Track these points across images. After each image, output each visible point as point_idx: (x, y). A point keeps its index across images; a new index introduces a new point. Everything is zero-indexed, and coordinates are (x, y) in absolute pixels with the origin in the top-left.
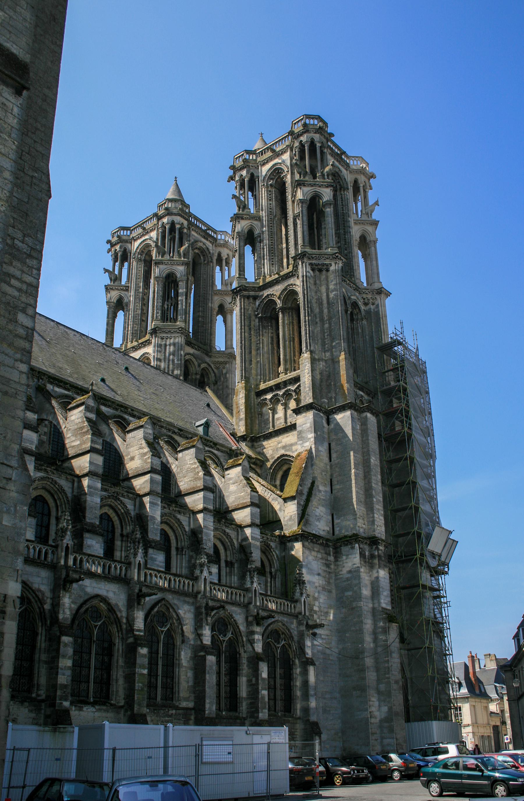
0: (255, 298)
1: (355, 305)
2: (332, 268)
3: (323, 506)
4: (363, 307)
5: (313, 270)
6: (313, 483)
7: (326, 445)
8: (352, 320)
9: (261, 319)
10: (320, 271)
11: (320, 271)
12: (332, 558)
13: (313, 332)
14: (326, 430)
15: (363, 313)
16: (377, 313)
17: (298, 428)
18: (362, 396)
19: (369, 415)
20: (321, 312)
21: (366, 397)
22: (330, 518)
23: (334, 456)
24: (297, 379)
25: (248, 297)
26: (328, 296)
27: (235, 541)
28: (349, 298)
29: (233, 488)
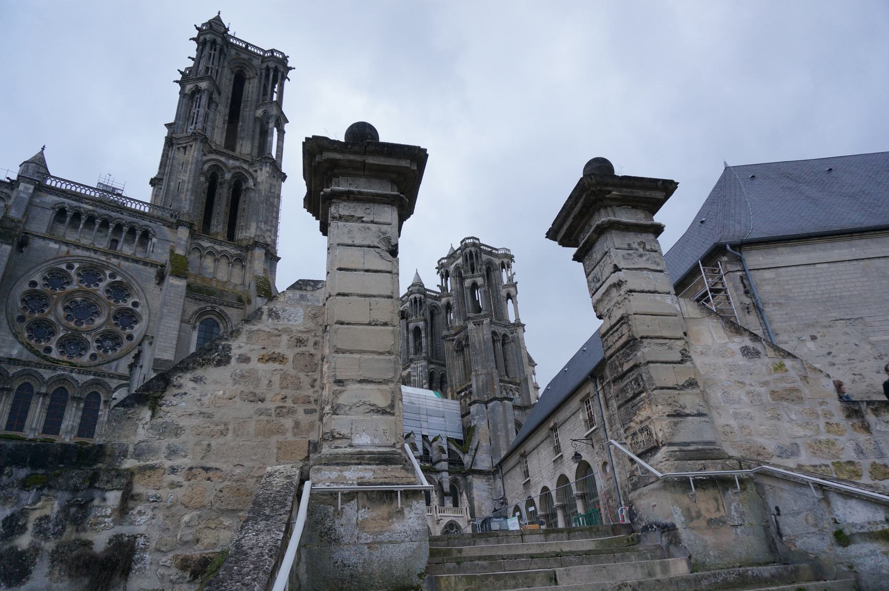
0: (453, 340)
1: (505, 336)
2: (484, 323)
3: (485, 453)
4: (510, 336)
5: (475, 325)
6: (479, 442)
7: (486, 420)
8: (504, 344)
9: (457, 351)
10: (479, 325)
11: (479, 325)
12: (492, 481)
13: (477, 360)
14: (485, 413)
15: (511, 339)
16: (518, 337)
17: (471, 414)
18: (511, 387)
19: (506, 401)
20: (480, 347)
21: (514, 387)
22: (490, 459)
23: (490, 426)
24: (471, 386)
25: (449, 341)
26: (483, 338)
27: (436, 480)
28: (500, 334)
29: (435, 452)
